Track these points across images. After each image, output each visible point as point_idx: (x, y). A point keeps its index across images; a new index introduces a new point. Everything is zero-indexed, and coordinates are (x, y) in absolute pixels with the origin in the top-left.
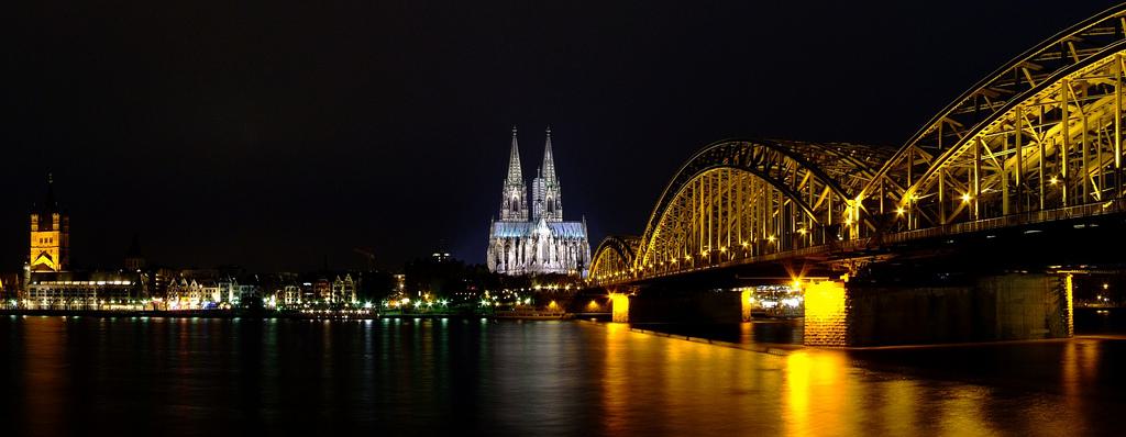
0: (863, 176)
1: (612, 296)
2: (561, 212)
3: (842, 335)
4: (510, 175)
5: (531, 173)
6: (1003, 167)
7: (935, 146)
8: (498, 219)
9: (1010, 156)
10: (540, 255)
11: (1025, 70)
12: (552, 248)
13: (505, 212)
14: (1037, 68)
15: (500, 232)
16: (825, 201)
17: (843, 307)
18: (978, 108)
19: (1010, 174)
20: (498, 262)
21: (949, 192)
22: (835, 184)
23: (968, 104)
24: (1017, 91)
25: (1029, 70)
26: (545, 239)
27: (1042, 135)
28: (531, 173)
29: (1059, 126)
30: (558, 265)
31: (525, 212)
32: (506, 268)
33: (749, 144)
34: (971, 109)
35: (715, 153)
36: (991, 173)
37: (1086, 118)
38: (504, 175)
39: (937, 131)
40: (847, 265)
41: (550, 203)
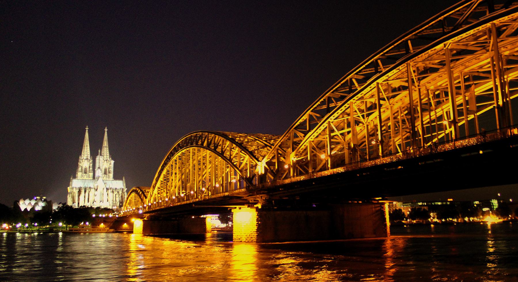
0: (268, 150)
1: (134, 220)
2: (111, 175)
4: (83, 153)
5: (95, 153)
6: (344, 140)
7: (304, 129)
8: (75, 177)
9: (349, 132)
11: (354, 80)
12: (105, 193)
13: (79, 174)
14: (361, 77)
15: (76, 184)
16: (246, 164)
18: (328, 105)
19: (349, 144)
21: (314, 156)
22: (251, 154)
23: (323, 103)
24: (350, 90)
25: (356, 80)
27: (366, 119)
28: (95, 153)
29: (376, 113)
31: (91, 174)
33: (207, 134)
34: (325, 107)
35: (189, 140)
36: (338, 143)
37: (391, 107)
38: (80, 153)
39: (305, 121)
40: (258, 199)
41: (106, 170)
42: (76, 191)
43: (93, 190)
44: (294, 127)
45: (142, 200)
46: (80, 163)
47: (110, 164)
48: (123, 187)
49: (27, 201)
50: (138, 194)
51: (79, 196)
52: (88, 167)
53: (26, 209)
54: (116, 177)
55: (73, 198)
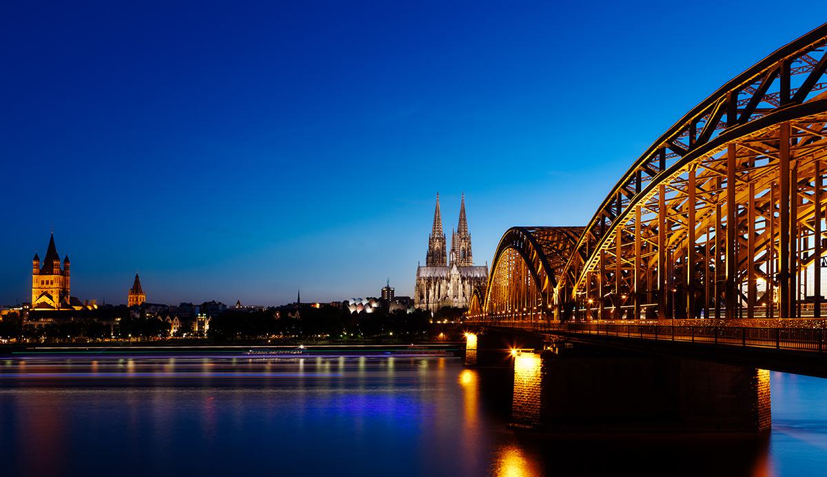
3: (538, 394)
10: (450, 292)
12: (461, 287)
17: (539, 373)
20: (422, 297)
26: (456, 280)
30: (464, 299)
43: (445, 281)
45: (481, 305)
47: (470, 243)
50: (478, 296)
51: (428, 290)
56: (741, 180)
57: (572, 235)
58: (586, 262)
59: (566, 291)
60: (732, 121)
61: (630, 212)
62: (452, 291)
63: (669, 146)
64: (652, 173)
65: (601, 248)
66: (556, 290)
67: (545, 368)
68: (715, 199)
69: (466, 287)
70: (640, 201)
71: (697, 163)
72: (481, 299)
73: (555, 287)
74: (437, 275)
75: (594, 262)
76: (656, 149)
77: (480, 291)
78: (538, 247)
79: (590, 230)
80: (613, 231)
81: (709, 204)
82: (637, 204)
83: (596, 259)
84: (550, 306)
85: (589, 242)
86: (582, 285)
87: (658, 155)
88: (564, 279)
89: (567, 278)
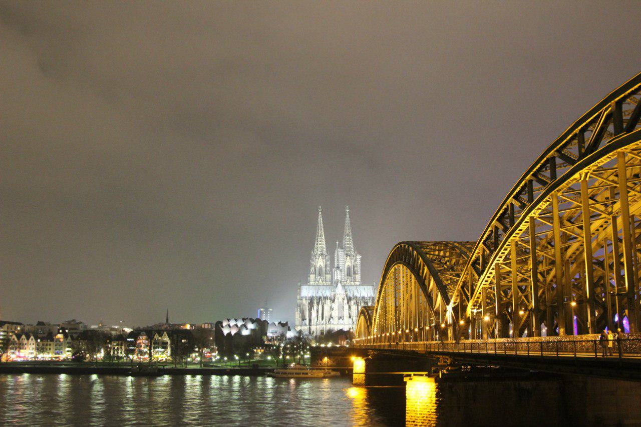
2: (358, 277)
8: (306, 282)
10: (335, 314)
12: (346, 307)
13: (312, 277)
15: (307, 292)
17: (434, 399)
20: (303, 319)
26: (341, 300)
30: (350, 320)
31: (328, 276)
32: (310, 325)
41: (349, 269)
42: (306, 303)
43: (328, 301)
44: (471, 263)
46: (313, 261)
48: (373, 295)
49: (232, 323)
50: (365, 317)
51: (310, 310)
52: (323, 265)
53: (229, 334)
54: (365, 282)
55: (302, 313)
56: (634, 190)
57: (465, 250)
58: (480, 276)
59: (459, 310)
60: (619, 130)
61: (523, 223)
62: (337, 312)
63: (559, 154)
64: (544, 183)
65: (495, 262)
66: (450, 308)
67: (441, 393)
68: (610, 210)
69: (352, 307)
70: (533, 211)
71: (588, 172)
72: (369, 321)
73: (448, 304)
74: (320, 294)
75: (489, 277)
76: (545, 159)
77: (367, 311)
78: (428, 263)
79: (484, 243)
80: (507, 243)
81: (603, 215)
82: (530, 215)
83: (491, 273)
84: (443, 326)
85: (483, 255)
86: (477, 302)
87: (548, 165)
88: (457, 296)
89: (461, 294)
